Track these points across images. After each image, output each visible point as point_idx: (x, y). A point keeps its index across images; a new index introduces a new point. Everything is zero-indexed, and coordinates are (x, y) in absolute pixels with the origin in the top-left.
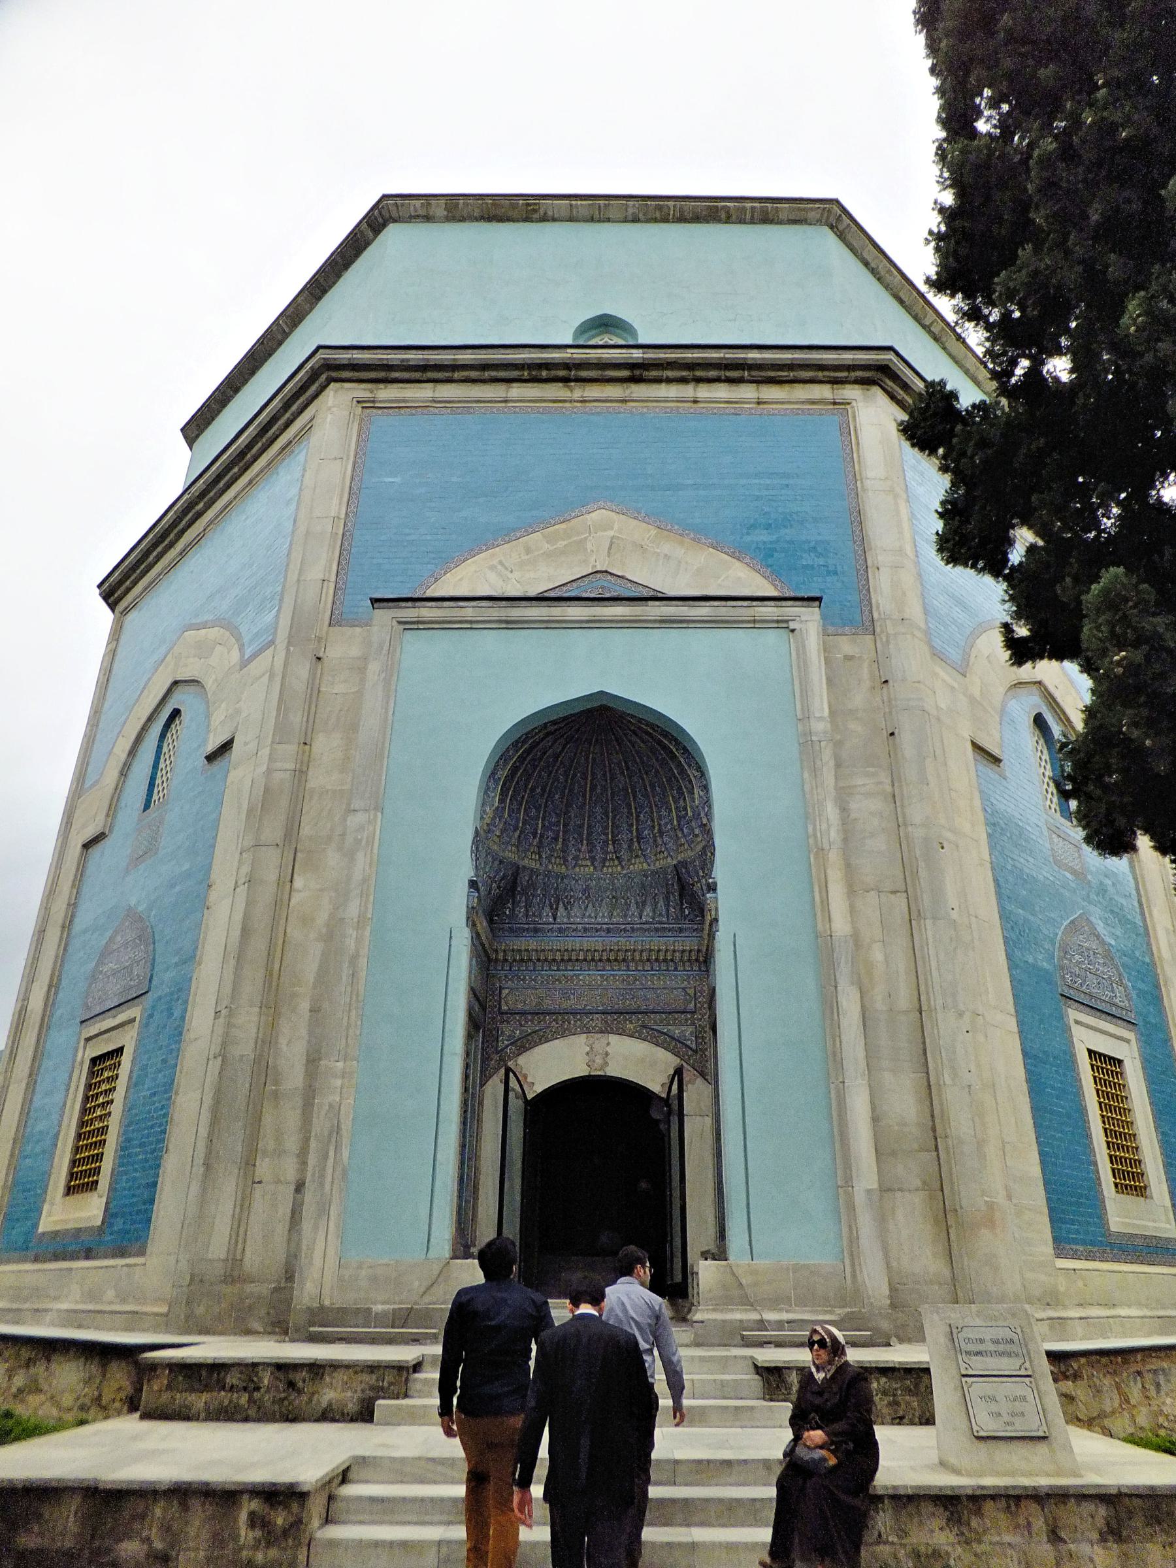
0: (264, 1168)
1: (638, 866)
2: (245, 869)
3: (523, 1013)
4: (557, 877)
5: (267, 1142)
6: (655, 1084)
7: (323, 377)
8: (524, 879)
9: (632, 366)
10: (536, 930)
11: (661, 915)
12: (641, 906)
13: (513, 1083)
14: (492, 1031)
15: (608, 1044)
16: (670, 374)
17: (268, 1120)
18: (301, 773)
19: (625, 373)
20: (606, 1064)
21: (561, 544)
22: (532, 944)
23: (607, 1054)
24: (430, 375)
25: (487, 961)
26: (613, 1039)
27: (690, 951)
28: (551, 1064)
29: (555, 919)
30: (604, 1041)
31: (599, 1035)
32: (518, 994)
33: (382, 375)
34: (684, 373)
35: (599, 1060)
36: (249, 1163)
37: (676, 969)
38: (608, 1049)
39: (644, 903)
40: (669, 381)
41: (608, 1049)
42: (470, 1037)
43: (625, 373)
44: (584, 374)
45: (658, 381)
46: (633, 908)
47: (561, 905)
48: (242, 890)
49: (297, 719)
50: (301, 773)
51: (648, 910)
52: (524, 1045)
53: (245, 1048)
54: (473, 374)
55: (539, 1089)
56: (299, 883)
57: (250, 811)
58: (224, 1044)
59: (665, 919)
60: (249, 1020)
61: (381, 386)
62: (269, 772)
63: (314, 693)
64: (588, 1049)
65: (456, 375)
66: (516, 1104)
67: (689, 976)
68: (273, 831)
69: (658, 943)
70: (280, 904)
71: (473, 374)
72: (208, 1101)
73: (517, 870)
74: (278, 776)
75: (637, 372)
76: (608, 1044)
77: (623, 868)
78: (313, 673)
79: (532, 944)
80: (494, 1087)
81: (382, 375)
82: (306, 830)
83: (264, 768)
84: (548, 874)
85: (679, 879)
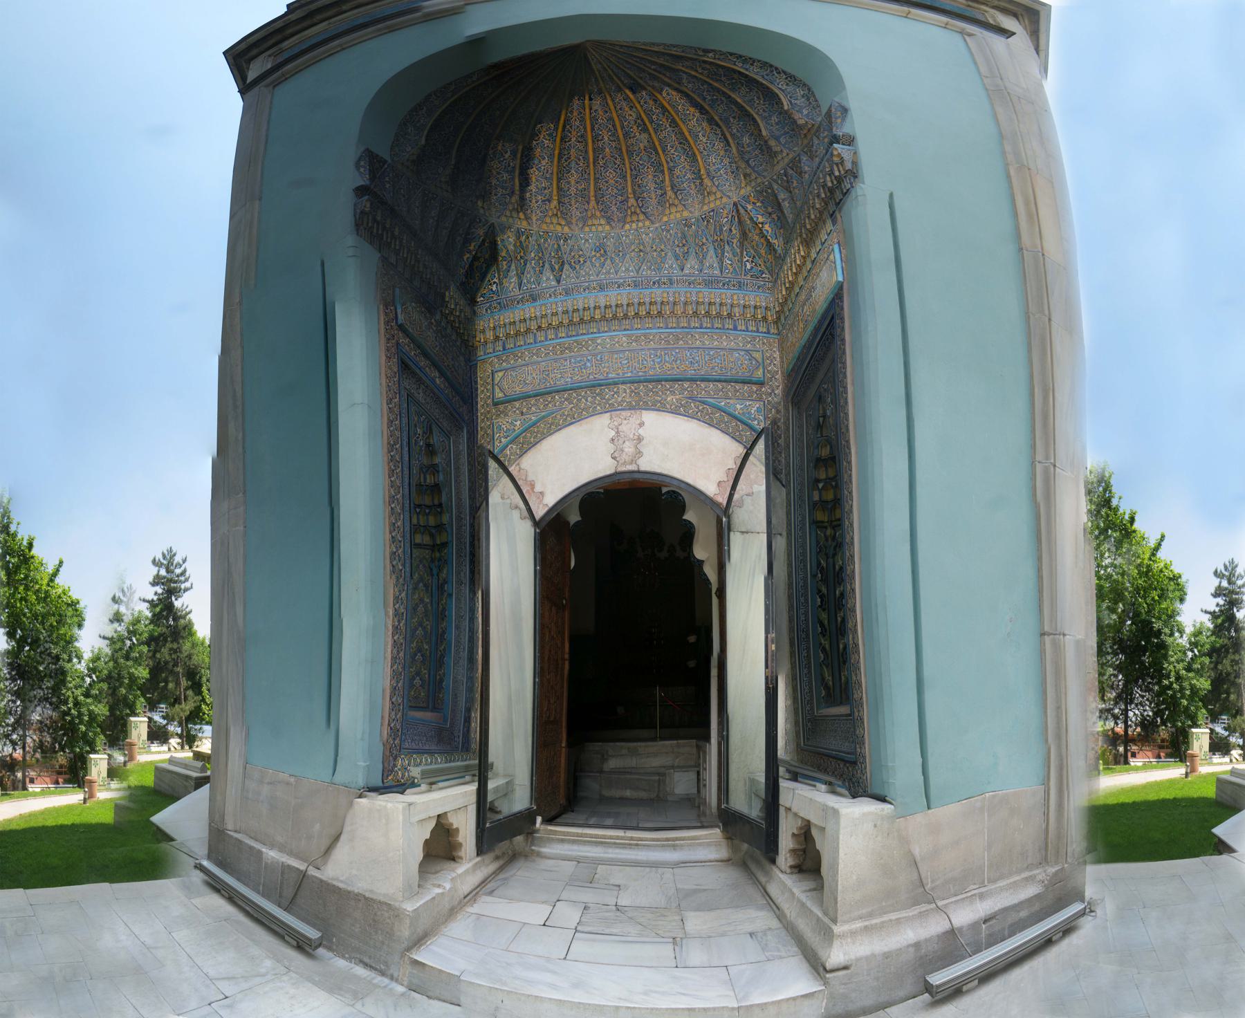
1: (675, 215)
11: (711, 267)
12: (682, 259)
15: (642, 424)
23: (640, 439)
26: (649, 417)
27: (755, 307)
31: (627, 413)
37: (735, 329)
38: (641, 431)
41: (641, 431)
46: (670, 261)
47: (566, 266)
59: (717, 272)
64: (613, 433)
67: (754, 338)
76: (642, 424)
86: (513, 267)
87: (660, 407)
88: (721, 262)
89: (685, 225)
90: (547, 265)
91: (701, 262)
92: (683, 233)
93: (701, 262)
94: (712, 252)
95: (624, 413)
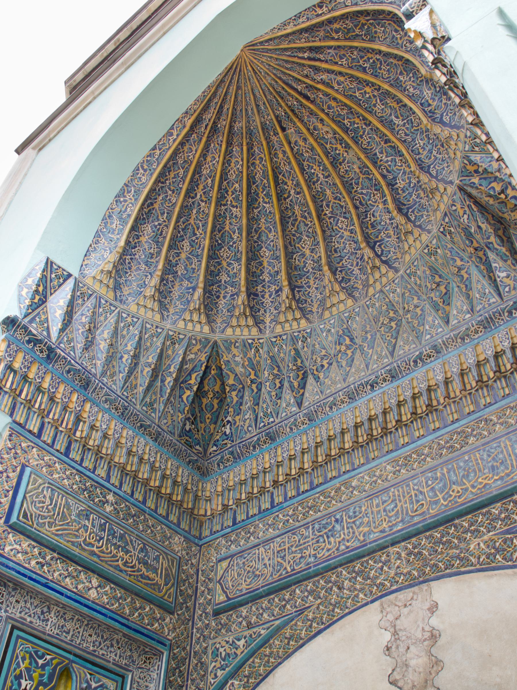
4: (294, 340)
10: (272, 438)
20: (437, 664)
23: (434, 637)
26: (443, 591)
29: (300, 405)
30: (418, 599)
31: (407, 594)
35: (417, 660)
38: (434, 622)
39: (447, 299)
47: (311, 380)
59: (495, 299)
64: (387, 636)
76: (434, 608)
77: (397, 270)
85: (483, 208)
86: (246, 398)
87: (459, 566)
88: (494, 282)
89: (430, 254)
90: (286, 384)
91: (468, 297)
92: (431, 268)
93: (468, 297)
94: (475, 273)
95: (402, 596)
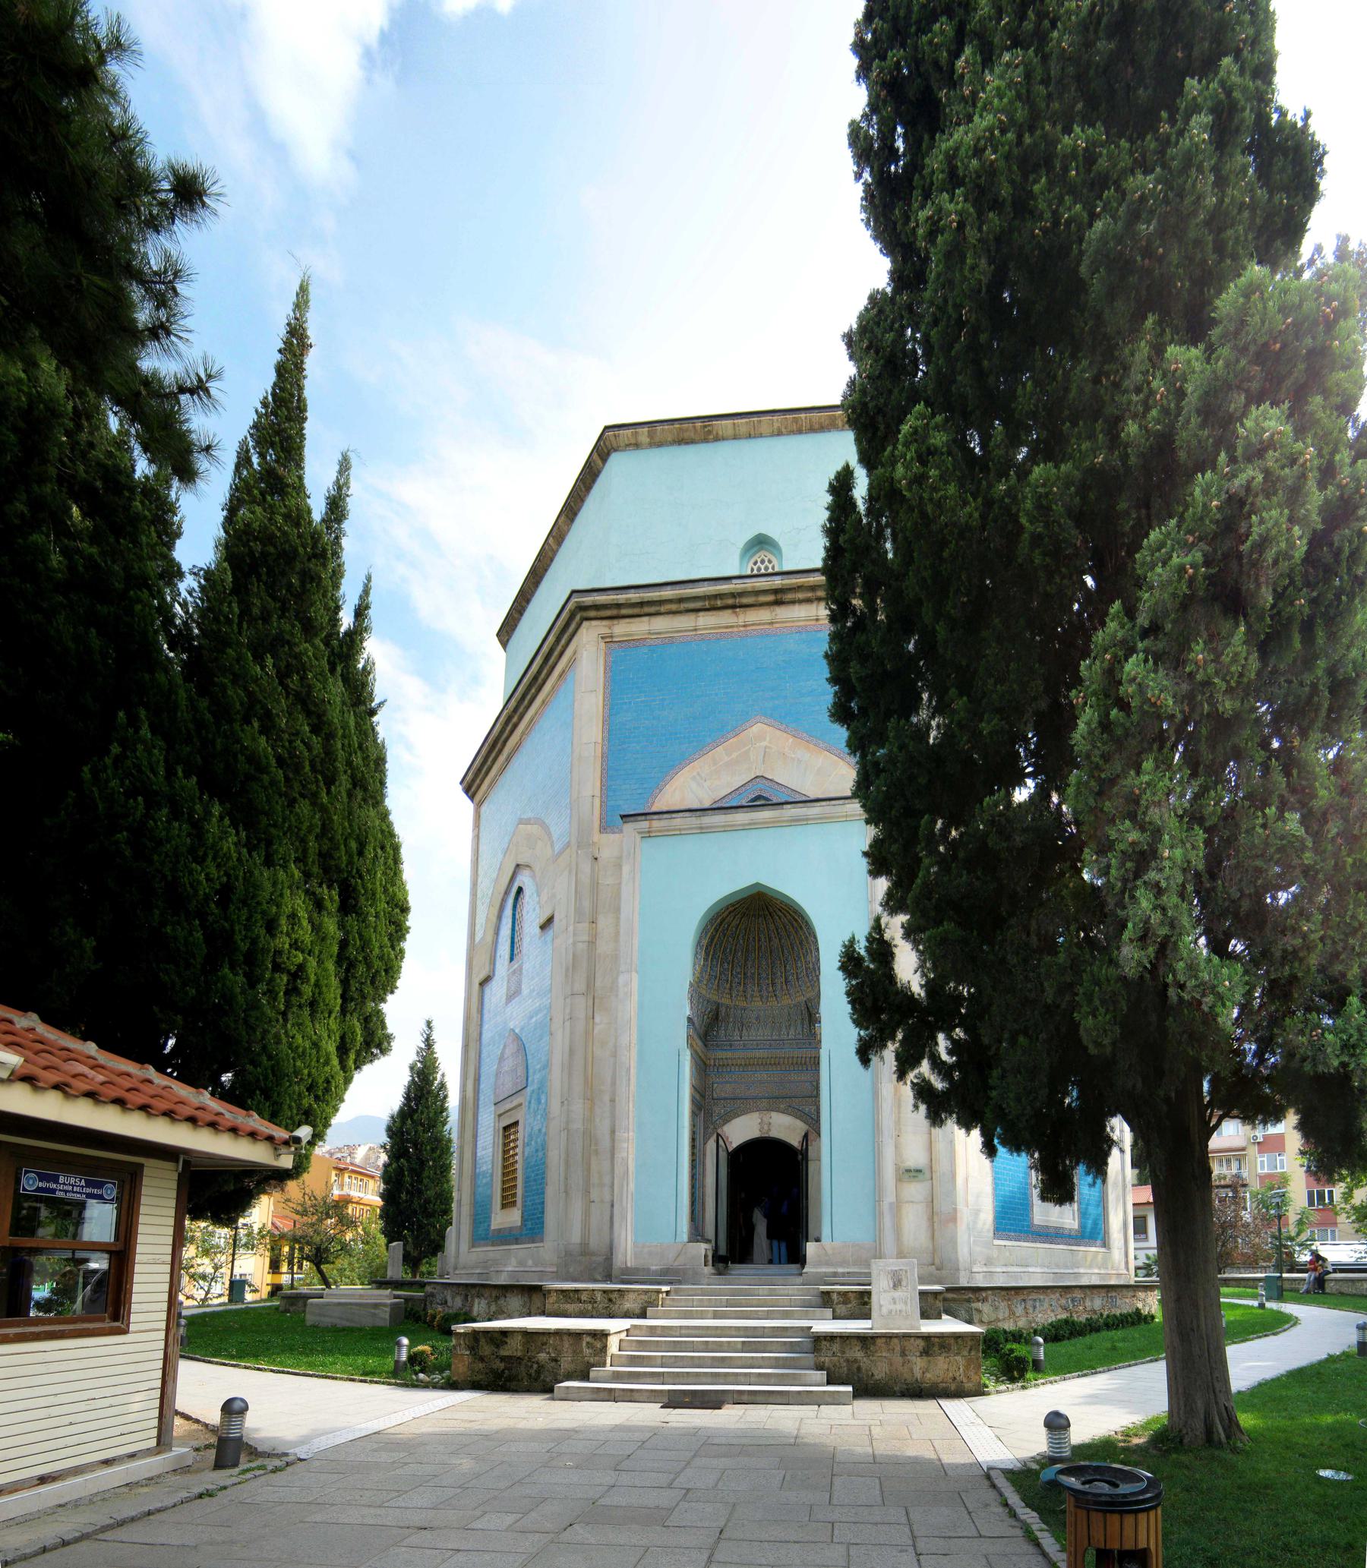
0: (594, 1194)
1: (786, 1001)
2: (568, 1011)
3: (725, 1099)
5: (595, 1179)
6: (795, 1141)
7: (578, 618)
8: (723, 1010)
9: (776, 591)
13: (721, 1142)
14: (707, 1109)
16: (800, 596)
17: (594, 1167)
18: (592, 943)
19: (770, 598)
21: (734, 755)
22: (729, 1054)
24: (647, 610)
25: (703, 1068)
26: (774, 1114)
28: (741, 1130)
32: (723, 1088)
33: (614, 612)
34: (810, 595)
36: (587, 1192)
40: (800, 602)
42: (694, 1114)
43: (770, 598)
44: (745, 601)
45: (793, 602)
48: (568, 1024)
49: (586, 904)
50: (592, 943)
51: (792, 1032)
52: (727, 1118)
53: (578, 1125)
54: (674, 607)
55: (735, 1145)
56: (597, 1019)
57: (567, 970)
58: (567, 1123)
60: (578, 1107)
61: (615, 622)
62: (574, 944)
63: (595, 886)
65: (663, 609)
66: (723, 1155)
68: (580, 986)
69: (797, 1053)
70: (588, 1033)
71: (674, 607)
72: (563, 1156)
73: (718, 1006)
74: (580, 946)
75: (779, 596)
78: (593, 870)
79: (729, 1054)
80: (711, 1145)
81: (614, 612)
82: (598, 984)
83: (571, 941)
84: (736, 1007)
87: (778, 1110)
